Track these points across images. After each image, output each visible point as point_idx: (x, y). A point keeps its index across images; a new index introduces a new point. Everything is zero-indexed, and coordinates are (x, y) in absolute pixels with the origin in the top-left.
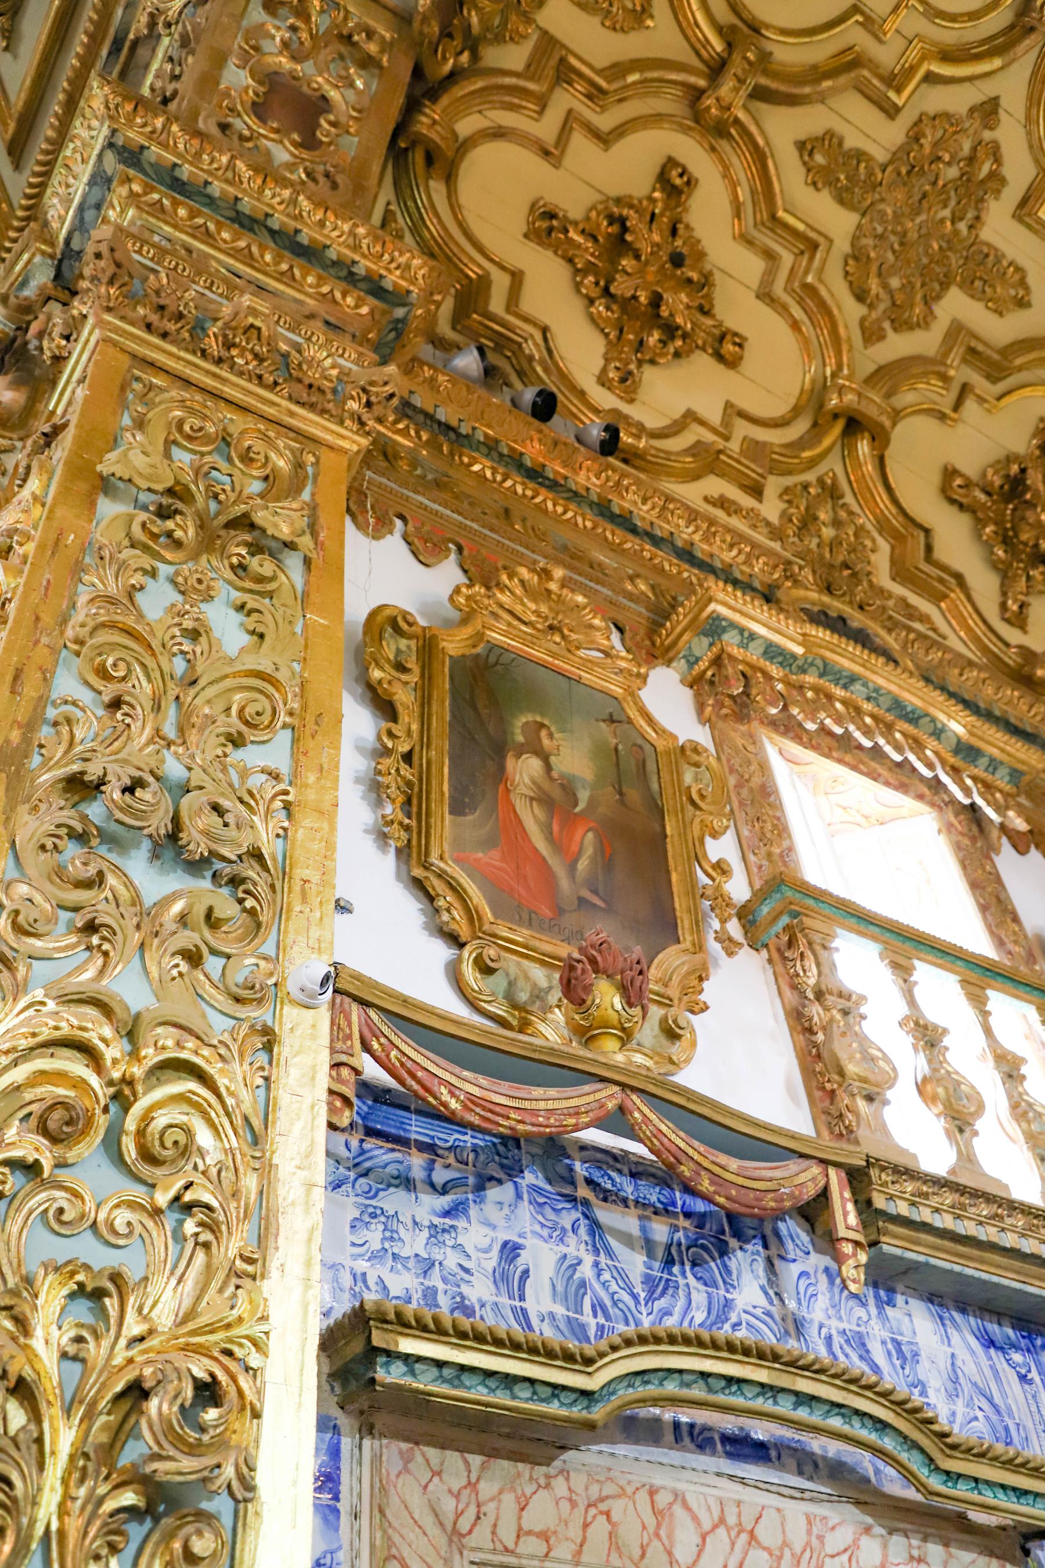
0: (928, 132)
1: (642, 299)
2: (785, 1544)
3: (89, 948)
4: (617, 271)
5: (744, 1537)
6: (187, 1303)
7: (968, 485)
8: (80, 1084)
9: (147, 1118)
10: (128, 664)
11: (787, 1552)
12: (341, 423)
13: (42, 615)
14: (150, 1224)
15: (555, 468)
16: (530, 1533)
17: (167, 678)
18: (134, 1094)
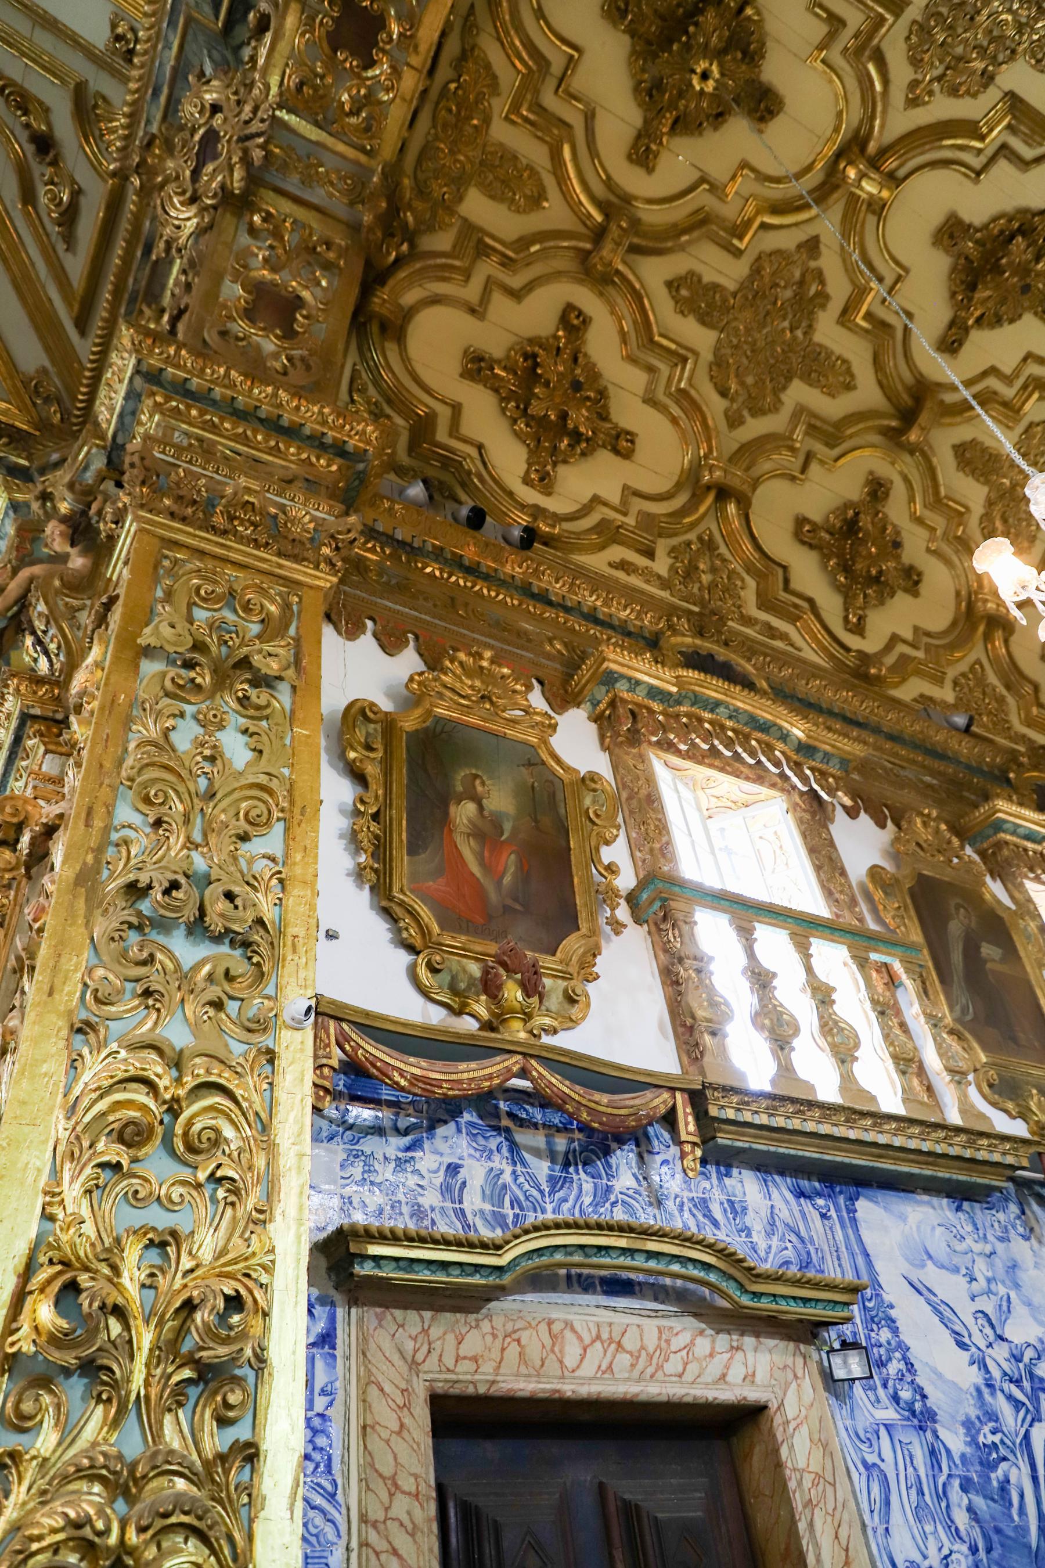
0: (767, 265)
2: (643, 1348)
3: (147, 1007)
5: (613, 1346)
6: (221, 1244)
8: (144, 1108)
9: (189, 1123)
10: (165, 793)
11: (643, 1353)
12: (317, 567)
13: (105, 763)
14: (195, 1193)
15: (489, 564)
16: (465, 1358)
17: (194, 796)
18: (181, 1108)
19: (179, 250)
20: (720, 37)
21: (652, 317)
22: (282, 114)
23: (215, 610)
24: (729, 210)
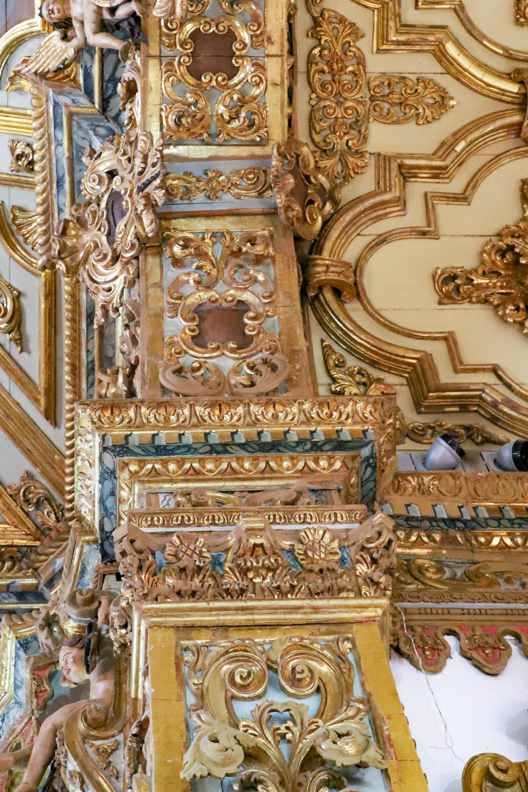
19: (116, 310)
22: (172, 150)
23: (259, 697)
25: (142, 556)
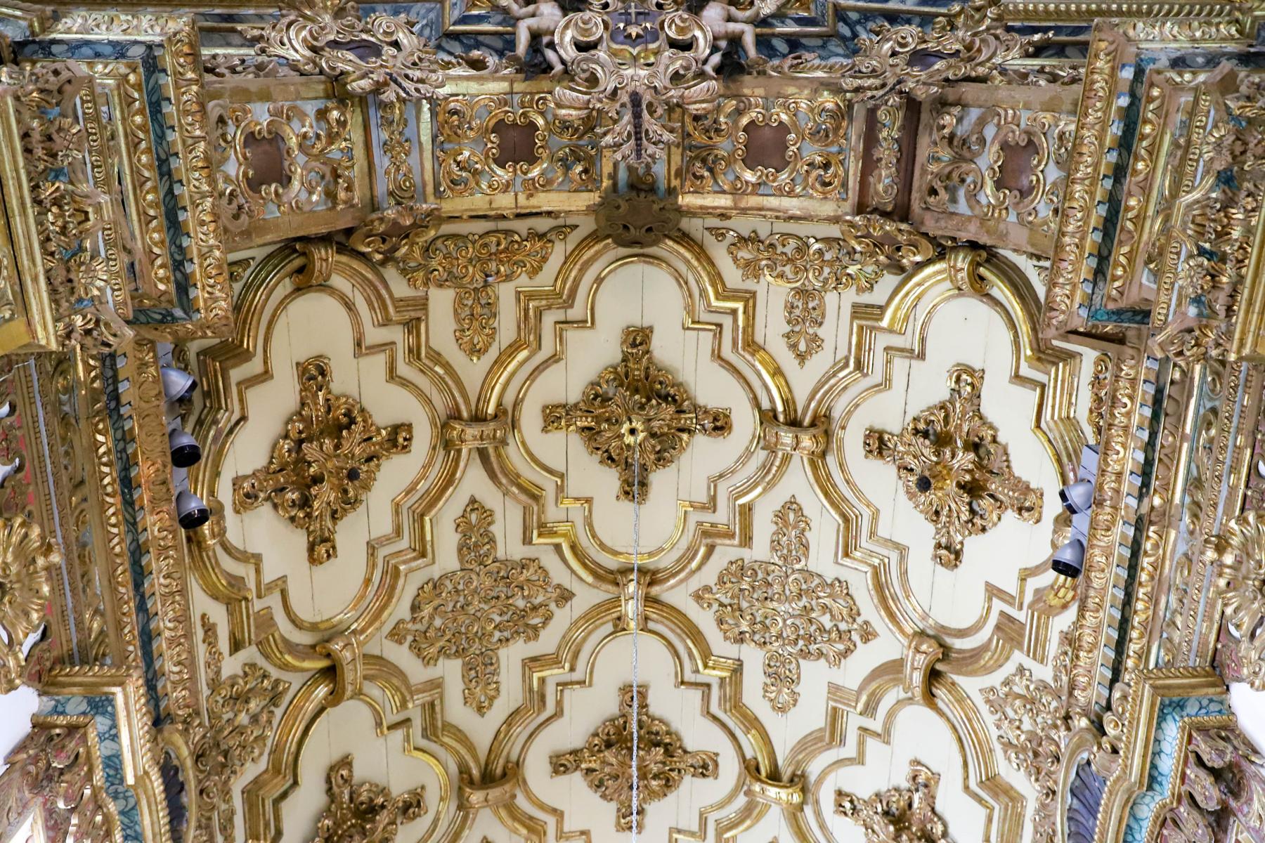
1: (312, 470)
4: (318, 440)
7: (346, 781)
12: (56, 320)
15: (144, 495)
20: (660, 427)
21: (441, 503)
22: (426, 106)
24: (553, 513)
25: (55, 93)
